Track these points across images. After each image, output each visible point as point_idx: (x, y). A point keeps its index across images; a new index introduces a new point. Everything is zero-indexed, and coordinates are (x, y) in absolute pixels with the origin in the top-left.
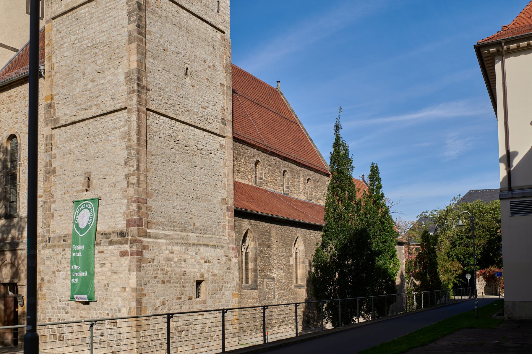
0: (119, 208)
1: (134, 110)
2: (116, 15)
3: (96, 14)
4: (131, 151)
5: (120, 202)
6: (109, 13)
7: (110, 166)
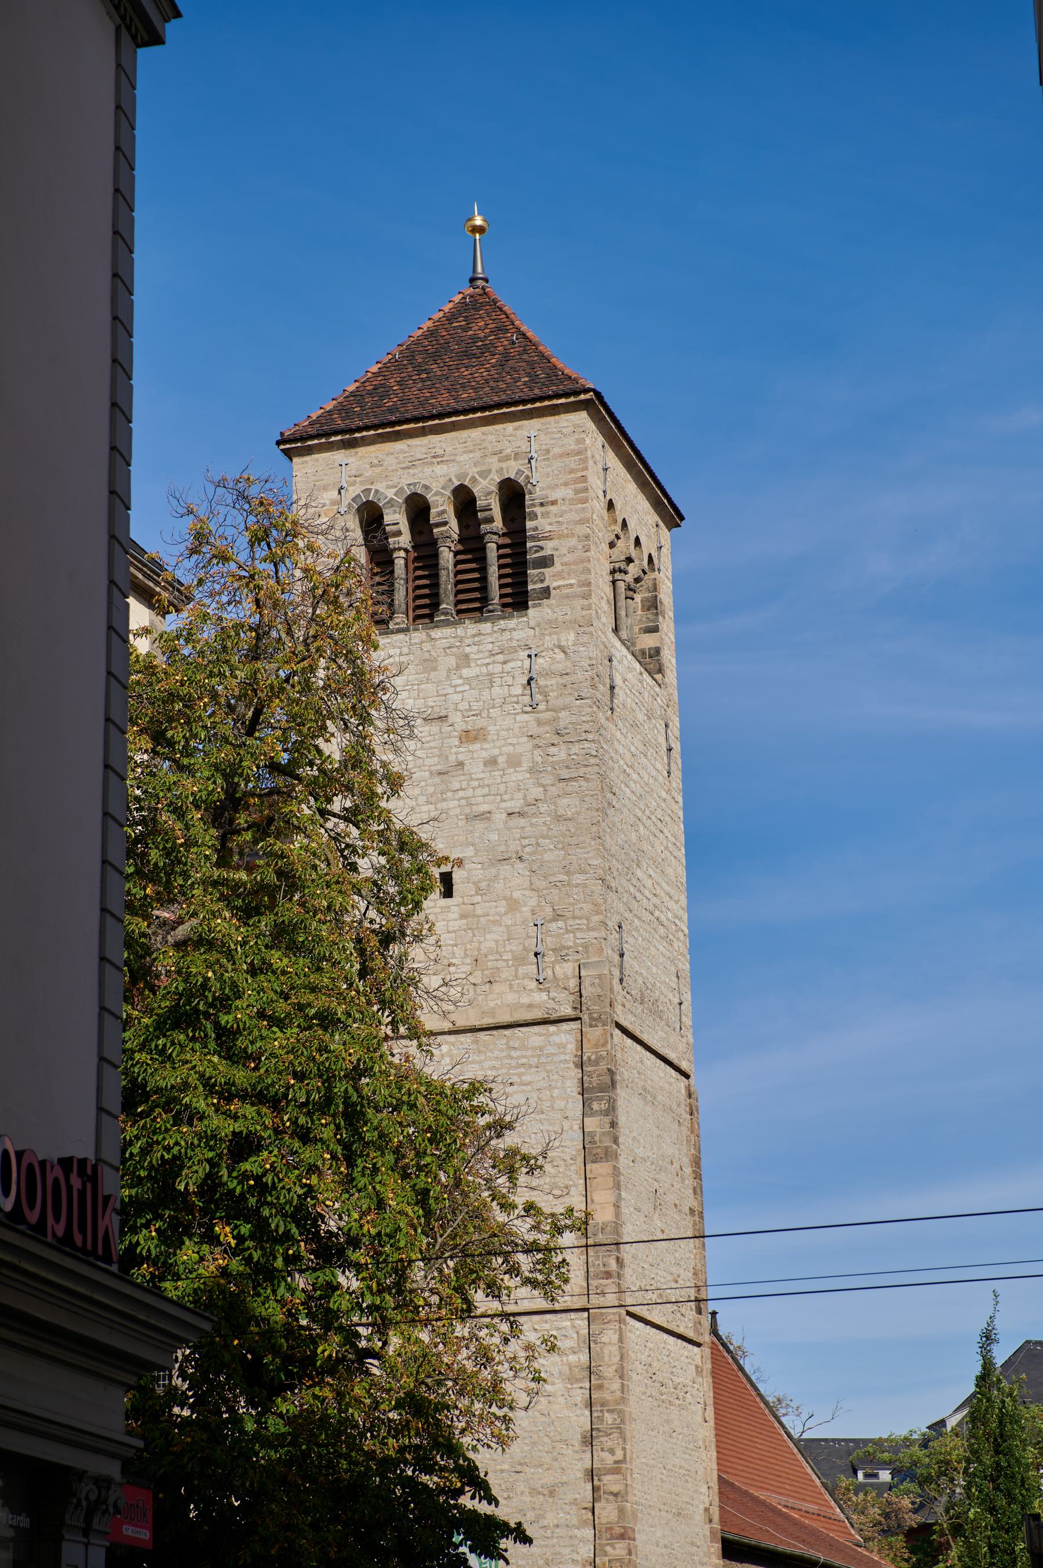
0: (569, 1550)
1: (609, 1318)
2: (542, 1084)
3: (477, 1066)
4: (606, 1415)
5: (570, 1533)
6: (520, 1075)
7: (534, 1443)
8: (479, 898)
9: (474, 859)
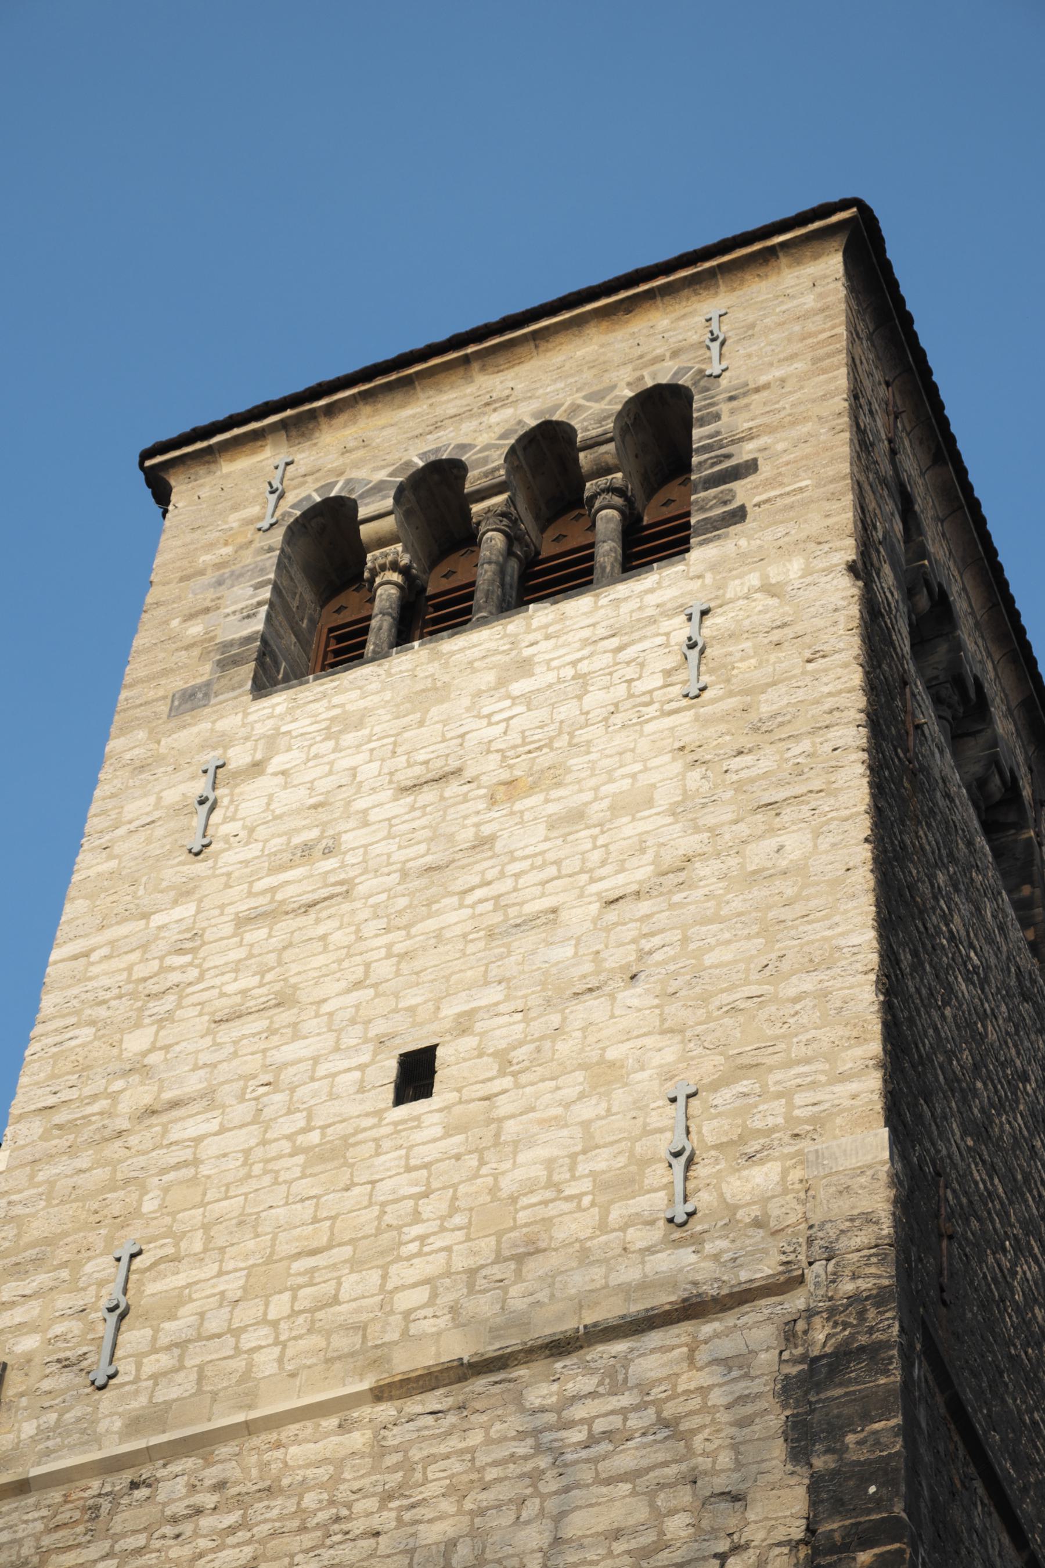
8: (507, 1082)
9: (501, 1008)
